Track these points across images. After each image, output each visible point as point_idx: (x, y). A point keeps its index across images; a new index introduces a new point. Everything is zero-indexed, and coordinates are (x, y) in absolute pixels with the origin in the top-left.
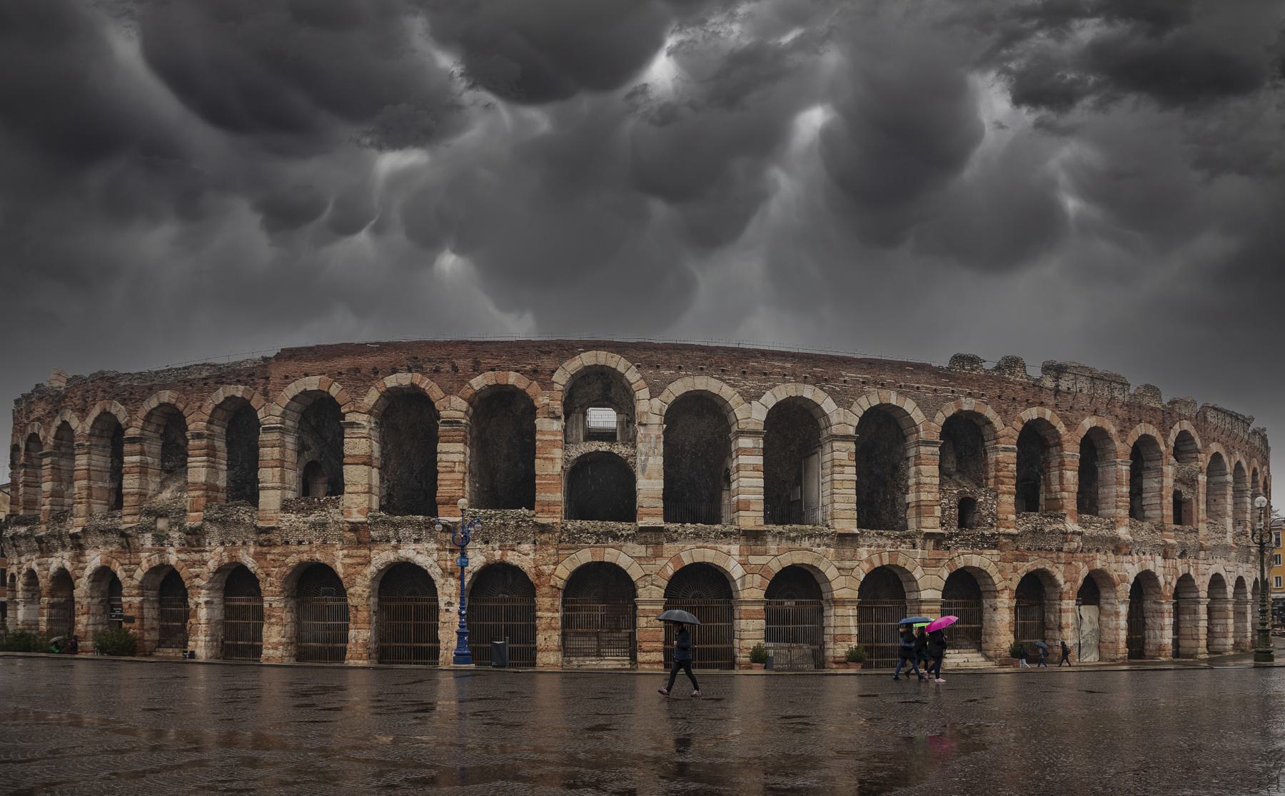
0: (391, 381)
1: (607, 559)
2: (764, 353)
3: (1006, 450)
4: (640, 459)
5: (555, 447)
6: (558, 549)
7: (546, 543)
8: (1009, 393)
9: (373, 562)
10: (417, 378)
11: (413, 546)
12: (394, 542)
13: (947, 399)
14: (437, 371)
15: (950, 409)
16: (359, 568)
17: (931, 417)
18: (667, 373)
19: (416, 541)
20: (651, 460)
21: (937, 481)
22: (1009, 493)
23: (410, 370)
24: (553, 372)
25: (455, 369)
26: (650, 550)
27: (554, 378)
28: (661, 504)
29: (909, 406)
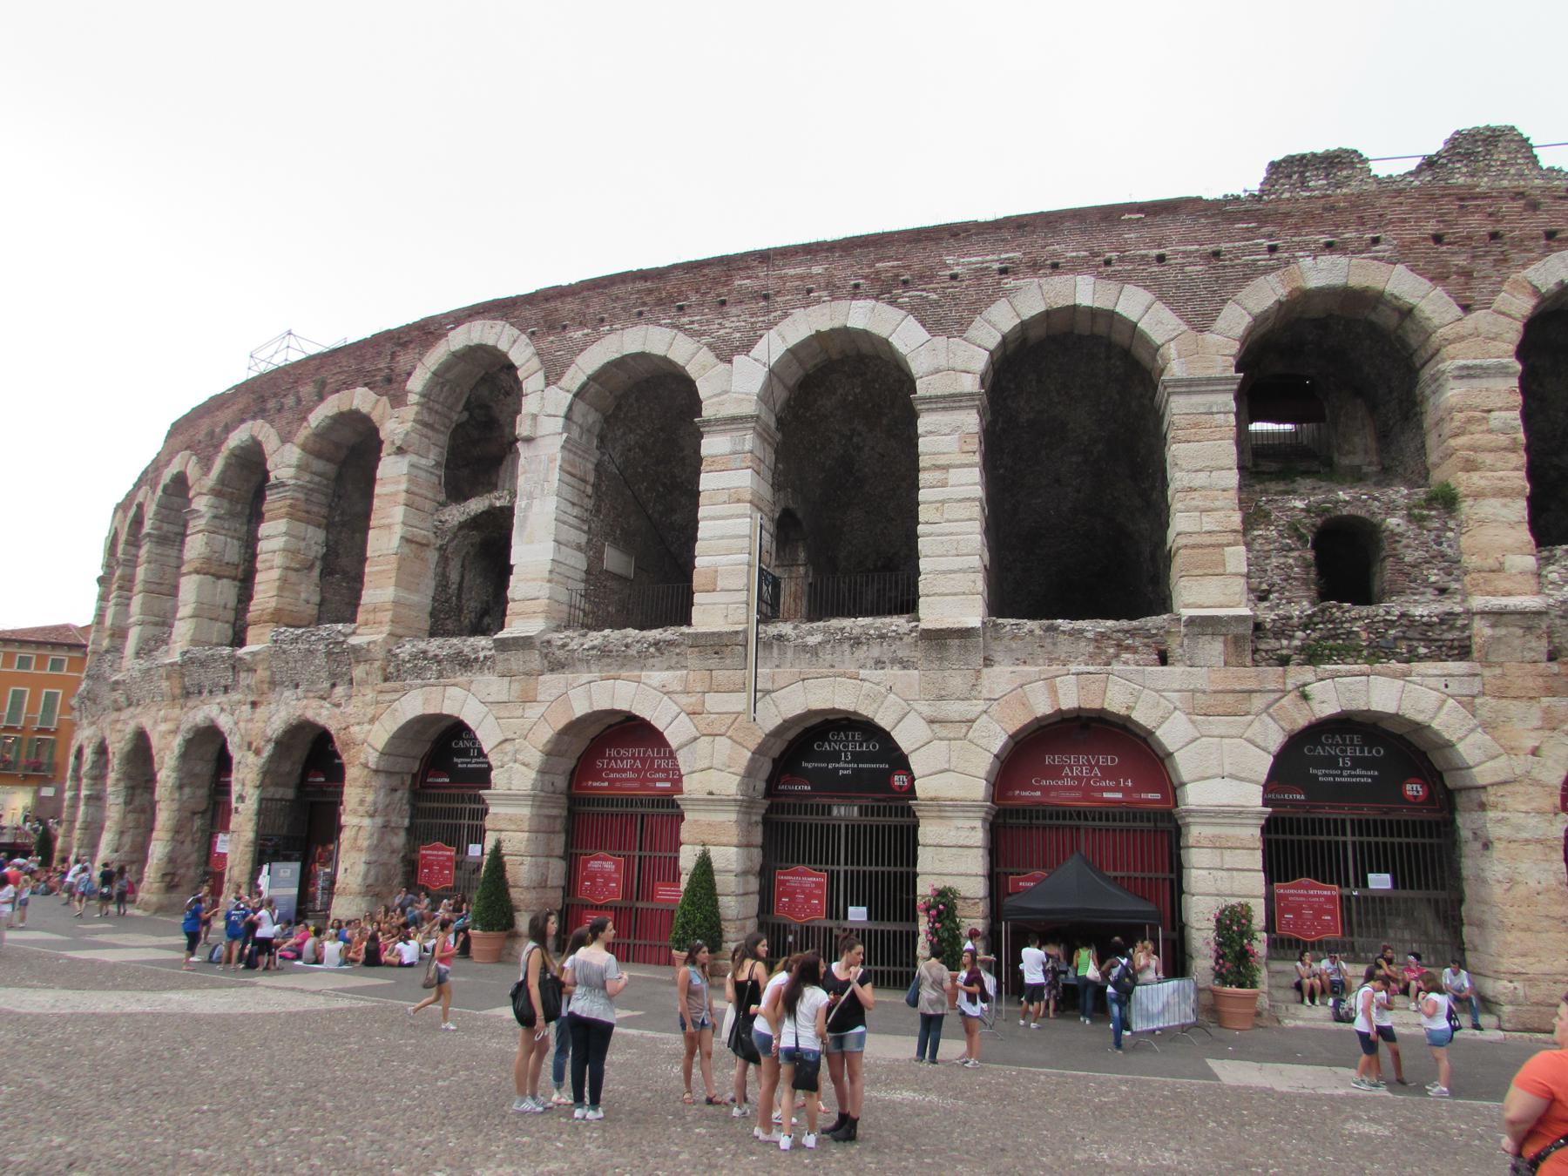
2: (765, 257)
3: (1467, 373)
5: (396, 503)
7: (363, 683)
8: (1477, 224)
11: (221, 698)
12: (205, 693)
13: (1251, 273)
15: (1265, 294)
16: (170, 738)
17: (1201, 322)
18: (579, 333)
19: (226, 689)
21: (1232, 478)
22: (1500, 493)
23: (254, 418)
24: (409, 374)
29: (1130, 301)
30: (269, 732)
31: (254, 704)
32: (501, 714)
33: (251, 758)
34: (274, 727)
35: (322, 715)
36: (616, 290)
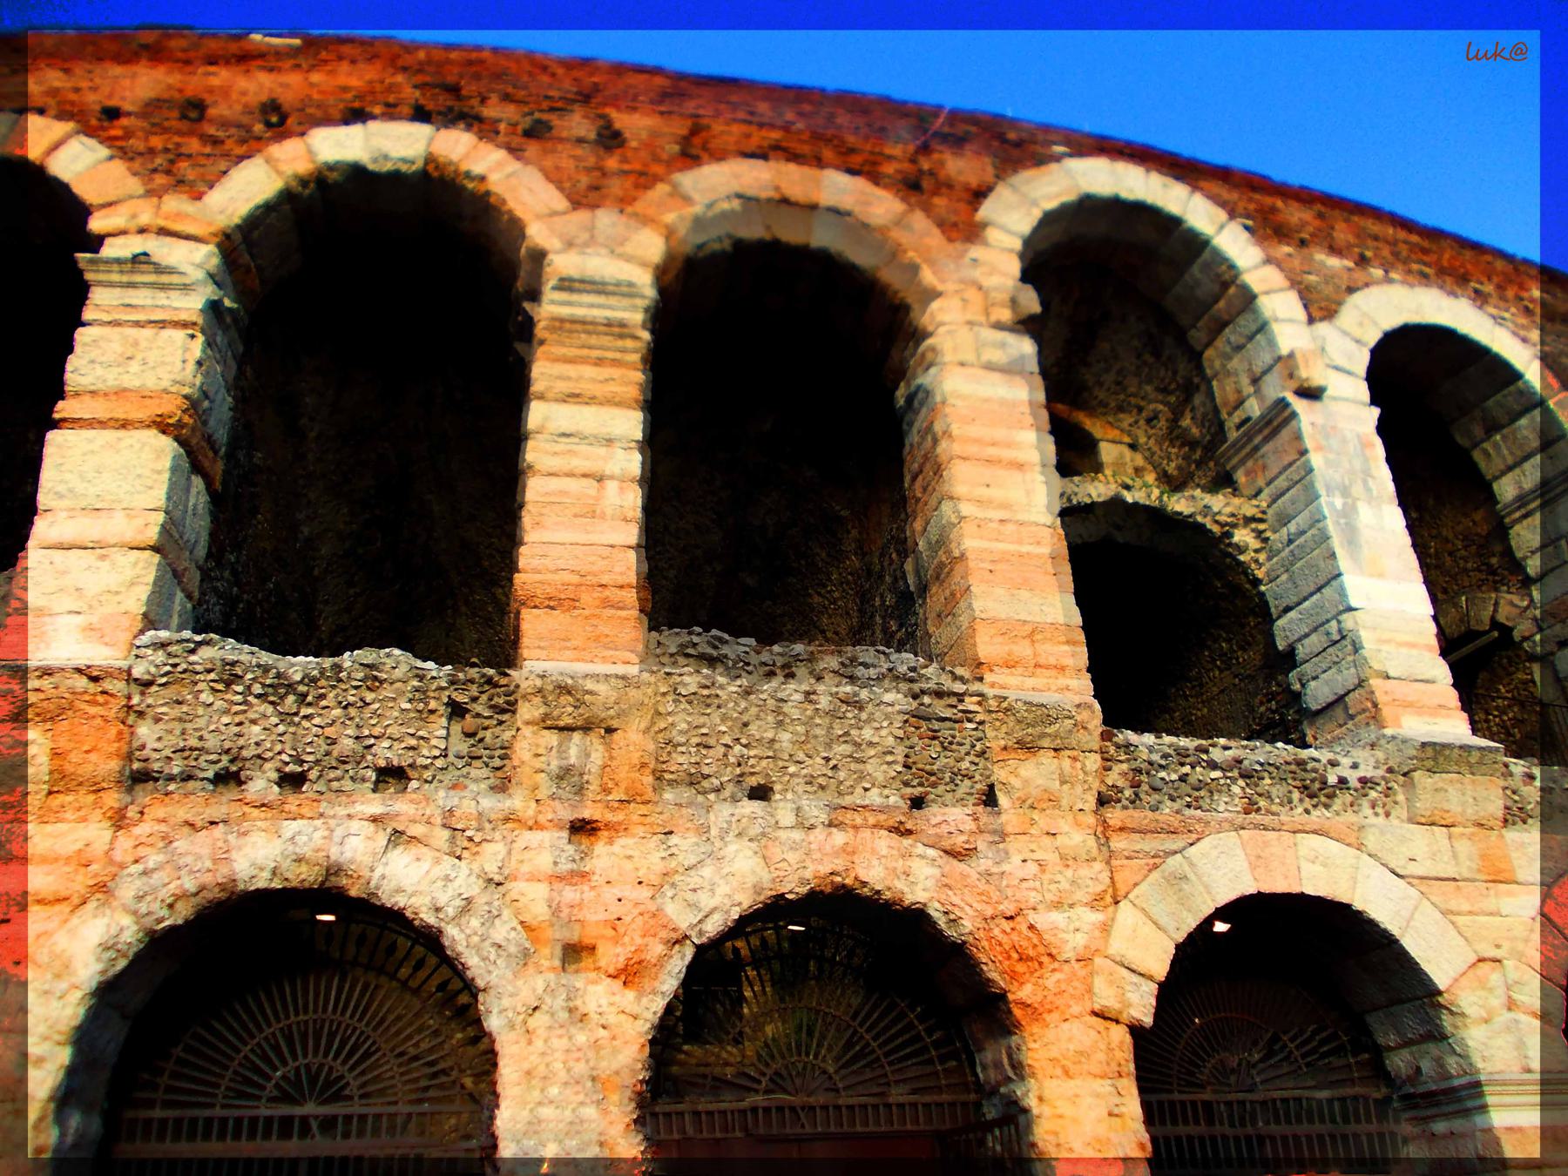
0: (338, 145)
1: (1315, 884)
4: (1330, 504)
6: (1105, 832)
9: (127, 890)
10: (458, 148)
11: (374, 805)
12: (261, 784)
14: (536, 132)
18: (1334, 262)
19: (393, 776)
20: (1365, 515)
24: (979, 194)
25: (611, 139)
26: (1463, 847)
27: (986, 210)
28: (1442, 672)
30: (683, 919)
31: (582, 829)
32: (1453, 905)
33: (599, 995)
34: (706, 901)
35: (908, 873)
36: (1373, 226)
